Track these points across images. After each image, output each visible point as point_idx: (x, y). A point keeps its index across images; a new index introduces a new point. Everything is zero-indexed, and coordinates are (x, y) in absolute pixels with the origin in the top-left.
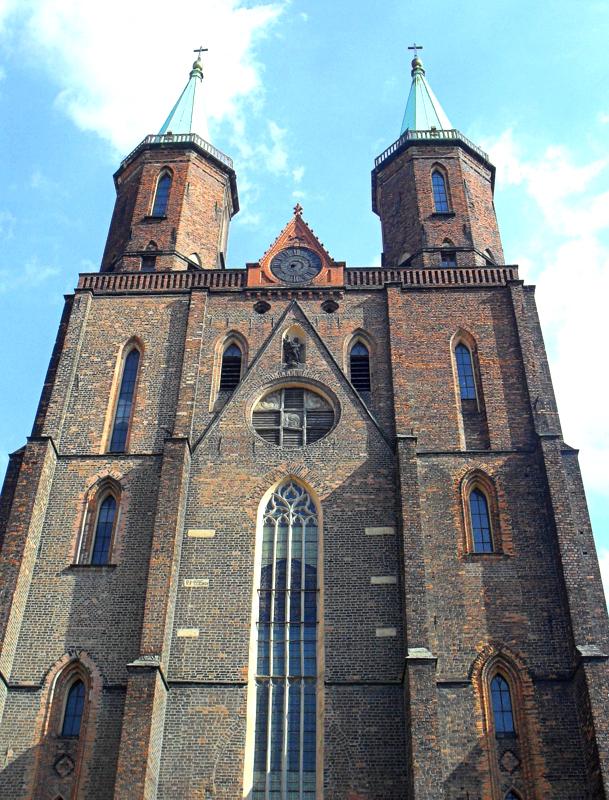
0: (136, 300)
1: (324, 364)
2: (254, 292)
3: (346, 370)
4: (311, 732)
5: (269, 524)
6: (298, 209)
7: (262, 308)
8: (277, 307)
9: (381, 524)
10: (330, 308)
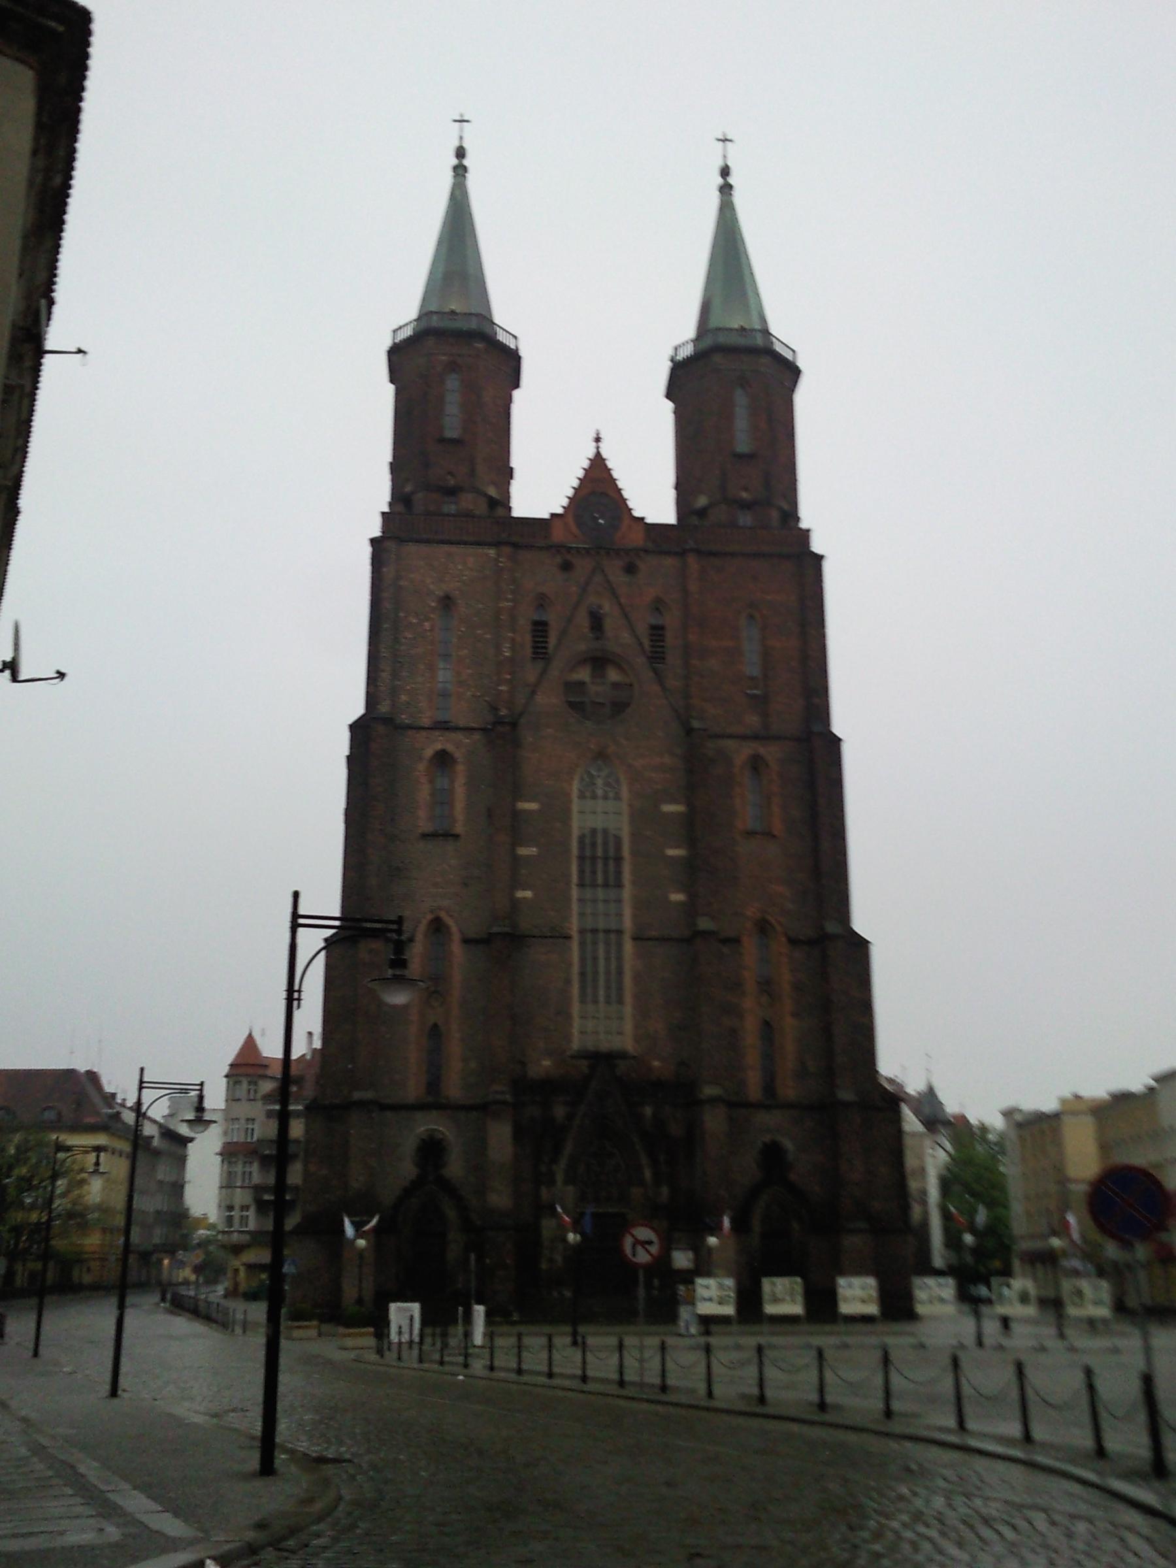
0: (446, 548)
1: (626, 637)
2: (559, 548)
3: (646, 642)
4: (620, 972)
5: (582, 796)
6: (598, 440)
7: (567, 567)
8: (583, 566)
9: (674, 801)
10: (630, 569)
